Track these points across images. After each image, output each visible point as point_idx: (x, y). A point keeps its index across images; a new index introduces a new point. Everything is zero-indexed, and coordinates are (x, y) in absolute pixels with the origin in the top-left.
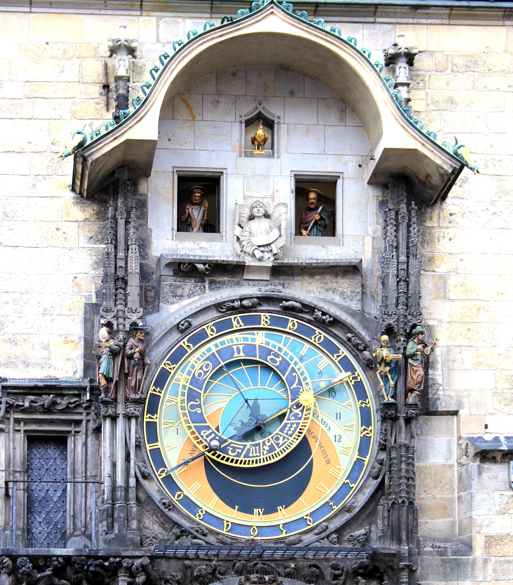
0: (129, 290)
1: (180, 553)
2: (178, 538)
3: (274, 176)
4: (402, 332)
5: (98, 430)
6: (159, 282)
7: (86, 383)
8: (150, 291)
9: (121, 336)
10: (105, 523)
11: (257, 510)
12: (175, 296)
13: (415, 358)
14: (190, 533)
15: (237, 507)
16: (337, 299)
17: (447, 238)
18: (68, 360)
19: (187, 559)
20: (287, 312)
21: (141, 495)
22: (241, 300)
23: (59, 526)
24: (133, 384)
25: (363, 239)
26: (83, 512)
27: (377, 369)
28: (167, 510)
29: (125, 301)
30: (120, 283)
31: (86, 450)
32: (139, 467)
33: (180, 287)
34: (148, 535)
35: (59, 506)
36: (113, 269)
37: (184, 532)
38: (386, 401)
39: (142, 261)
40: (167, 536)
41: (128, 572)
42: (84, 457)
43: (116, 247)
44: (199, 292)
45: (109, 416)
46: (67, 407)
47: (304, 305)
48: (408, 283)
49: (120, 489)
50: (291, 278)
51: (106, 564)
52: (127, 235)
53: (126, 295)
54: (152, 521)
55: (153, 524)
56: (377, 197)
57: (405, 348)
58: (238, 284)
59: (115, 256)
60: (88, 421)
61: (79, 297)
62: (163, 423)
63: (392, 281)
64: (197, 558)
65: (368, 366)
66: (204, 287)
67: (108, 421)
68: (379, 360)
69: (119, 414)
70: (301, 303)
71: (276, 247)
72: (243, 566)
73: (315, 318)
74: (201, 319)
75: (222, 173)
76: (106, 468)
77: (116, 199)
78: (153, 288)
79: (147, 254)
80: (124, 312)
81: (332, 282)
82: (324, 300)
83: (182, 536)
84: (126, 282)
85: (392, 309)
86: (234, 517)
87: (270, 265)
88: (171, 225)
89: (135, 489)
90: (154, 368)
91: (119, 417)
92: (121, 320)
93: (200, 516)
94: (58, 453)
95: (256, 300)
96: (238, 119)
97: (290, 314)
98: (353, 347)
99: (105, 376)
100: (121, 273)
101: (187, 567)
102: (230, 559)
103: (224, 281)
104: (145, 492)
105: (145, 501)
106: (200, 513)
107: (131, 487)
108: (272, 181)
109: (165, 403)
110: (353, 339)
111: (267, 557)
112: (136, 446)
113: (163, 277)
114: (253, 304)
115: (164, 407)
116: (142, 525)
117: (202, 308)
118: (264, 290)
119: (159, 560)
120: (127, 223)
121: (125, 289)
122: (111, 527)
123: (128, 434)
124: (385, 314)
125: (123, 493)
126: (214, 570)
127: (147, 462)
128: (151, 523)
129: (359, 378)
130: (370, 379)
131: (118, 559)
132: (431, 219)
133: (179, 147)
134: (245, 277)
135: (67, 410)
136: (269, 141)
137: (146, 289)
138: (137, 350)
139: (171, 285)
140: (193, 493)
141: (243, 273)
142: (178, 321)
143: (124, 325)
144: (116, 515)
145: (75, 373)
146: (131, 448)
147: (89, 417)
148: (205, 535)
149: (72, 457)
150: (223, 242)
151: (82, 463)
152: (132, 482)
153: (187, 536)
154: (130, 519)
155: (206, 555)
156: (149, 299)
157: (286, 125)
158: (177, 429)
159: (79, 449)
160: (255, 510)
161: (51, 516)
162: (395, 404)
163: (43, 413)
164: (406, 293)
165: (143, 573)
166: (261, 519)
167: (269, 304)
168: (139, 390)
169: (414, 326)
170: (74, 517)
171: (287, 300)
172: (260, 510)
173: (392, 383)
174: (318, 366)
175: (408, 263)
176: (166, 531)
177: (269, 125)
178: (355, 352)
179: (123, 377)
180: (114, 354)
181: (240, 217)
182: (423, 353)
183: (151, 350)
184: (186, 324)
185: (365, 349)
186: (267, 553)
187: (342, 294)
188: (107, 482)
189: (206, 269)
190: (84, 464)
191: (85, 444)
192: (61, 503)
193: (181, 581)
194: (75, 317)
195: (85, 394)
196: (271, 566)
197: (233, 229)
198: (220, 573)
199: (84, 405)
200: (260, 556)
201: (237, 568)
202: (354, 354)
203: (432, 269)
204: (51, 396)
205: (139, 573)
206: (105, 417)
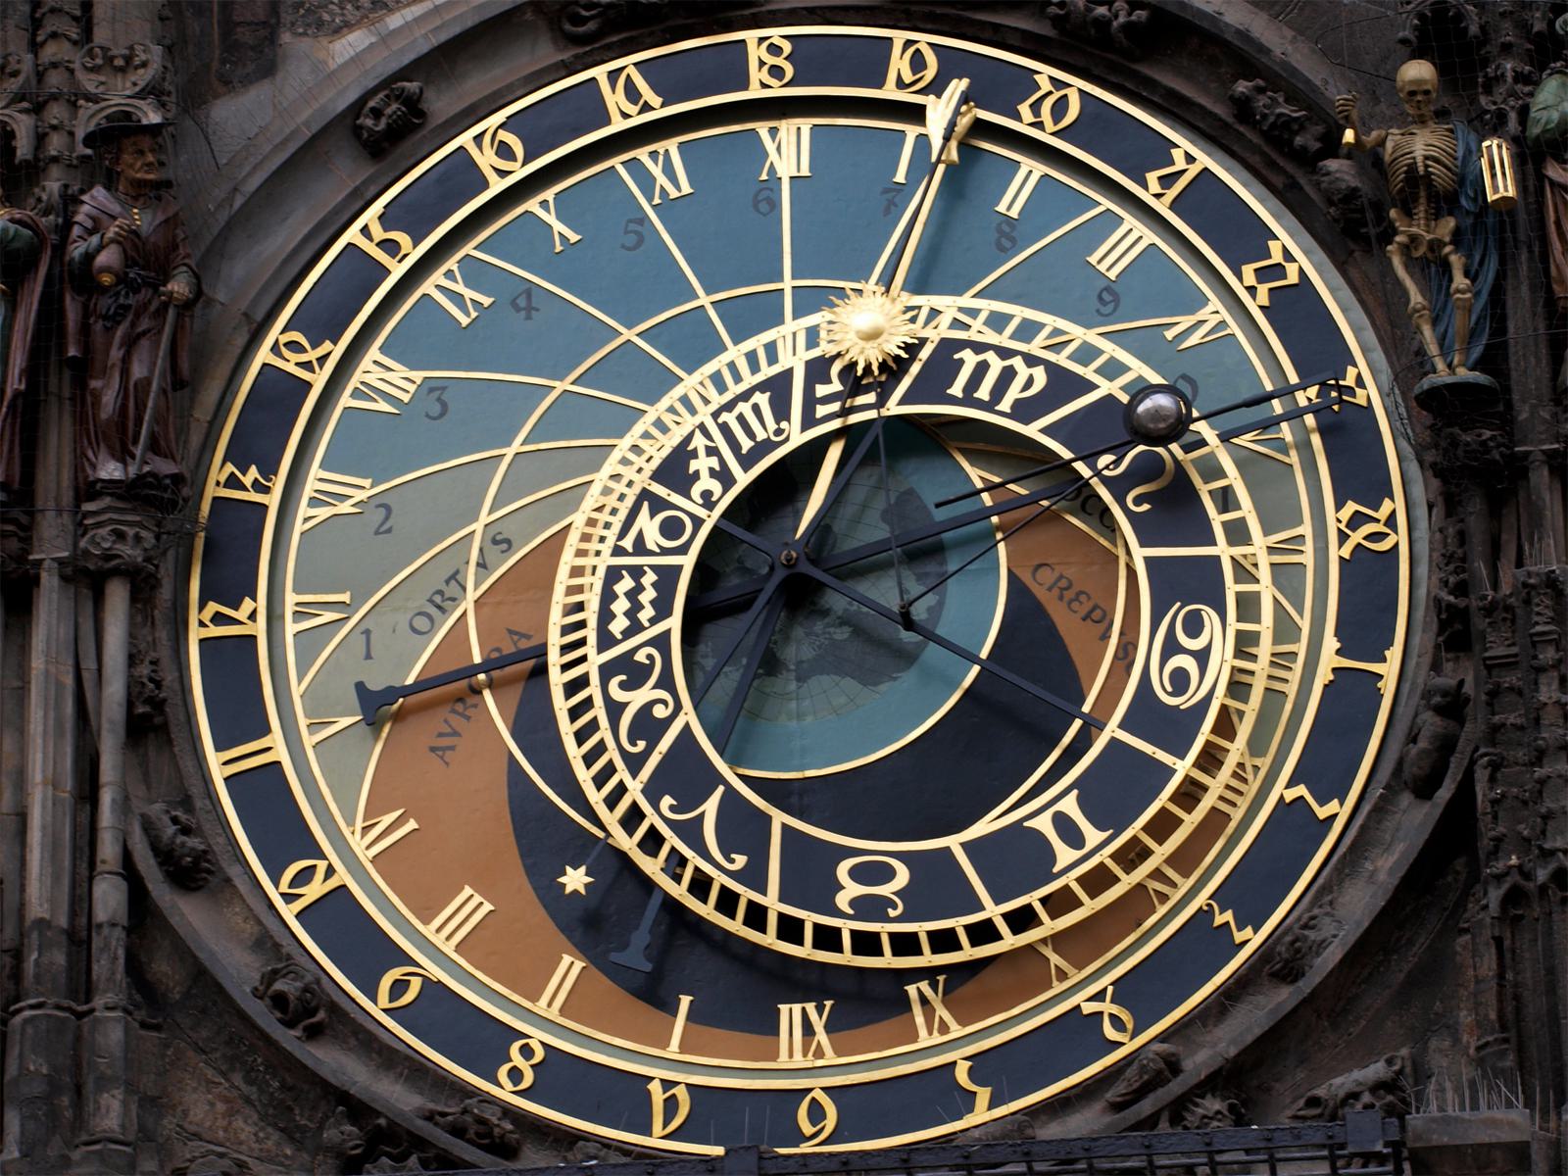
4: (1508, 34)
9: (52, 186)
11: (797, 1008)
14: (419, 1143)
15: (685, 1001)
21: (164, 969)
27: (1388, 234)
32: (148, 826)
49: (35, 935)
54: (227, 1100)
55: (230, 1113)
89: (119, 934)
90: (241, 340)
91: (36, 581)
92: (56, 112)
93: (515, 1075)
98: (1266, 149)
104: (183, 952)
106: (517, 1060)
107: (100, 926)
109: (303, 510)
110: (1262, 101)
115: (299, 527)
116: (168, 1123)
117: (470, 24)
123: (89, 664)
125: (59, 958)
127: (198, 804)
128: (220, 1107)
129: (1292, 270)
130: (1370, 299)
140: (449, 949)
142: (352, 96)
143: (71, 134)
146: (105, 726)
152: (109, 898)
154: (89, 1086)
156: (244, 35)
158: (367, 632)
160: (784, 1008)
166: (819, 1053)
172: (811, 1007)
174: (1093, 259)
178: (1282, 171)
179: (59, 383)
183: (219, 248)
184: (394, 106)
202: (1279, 181)
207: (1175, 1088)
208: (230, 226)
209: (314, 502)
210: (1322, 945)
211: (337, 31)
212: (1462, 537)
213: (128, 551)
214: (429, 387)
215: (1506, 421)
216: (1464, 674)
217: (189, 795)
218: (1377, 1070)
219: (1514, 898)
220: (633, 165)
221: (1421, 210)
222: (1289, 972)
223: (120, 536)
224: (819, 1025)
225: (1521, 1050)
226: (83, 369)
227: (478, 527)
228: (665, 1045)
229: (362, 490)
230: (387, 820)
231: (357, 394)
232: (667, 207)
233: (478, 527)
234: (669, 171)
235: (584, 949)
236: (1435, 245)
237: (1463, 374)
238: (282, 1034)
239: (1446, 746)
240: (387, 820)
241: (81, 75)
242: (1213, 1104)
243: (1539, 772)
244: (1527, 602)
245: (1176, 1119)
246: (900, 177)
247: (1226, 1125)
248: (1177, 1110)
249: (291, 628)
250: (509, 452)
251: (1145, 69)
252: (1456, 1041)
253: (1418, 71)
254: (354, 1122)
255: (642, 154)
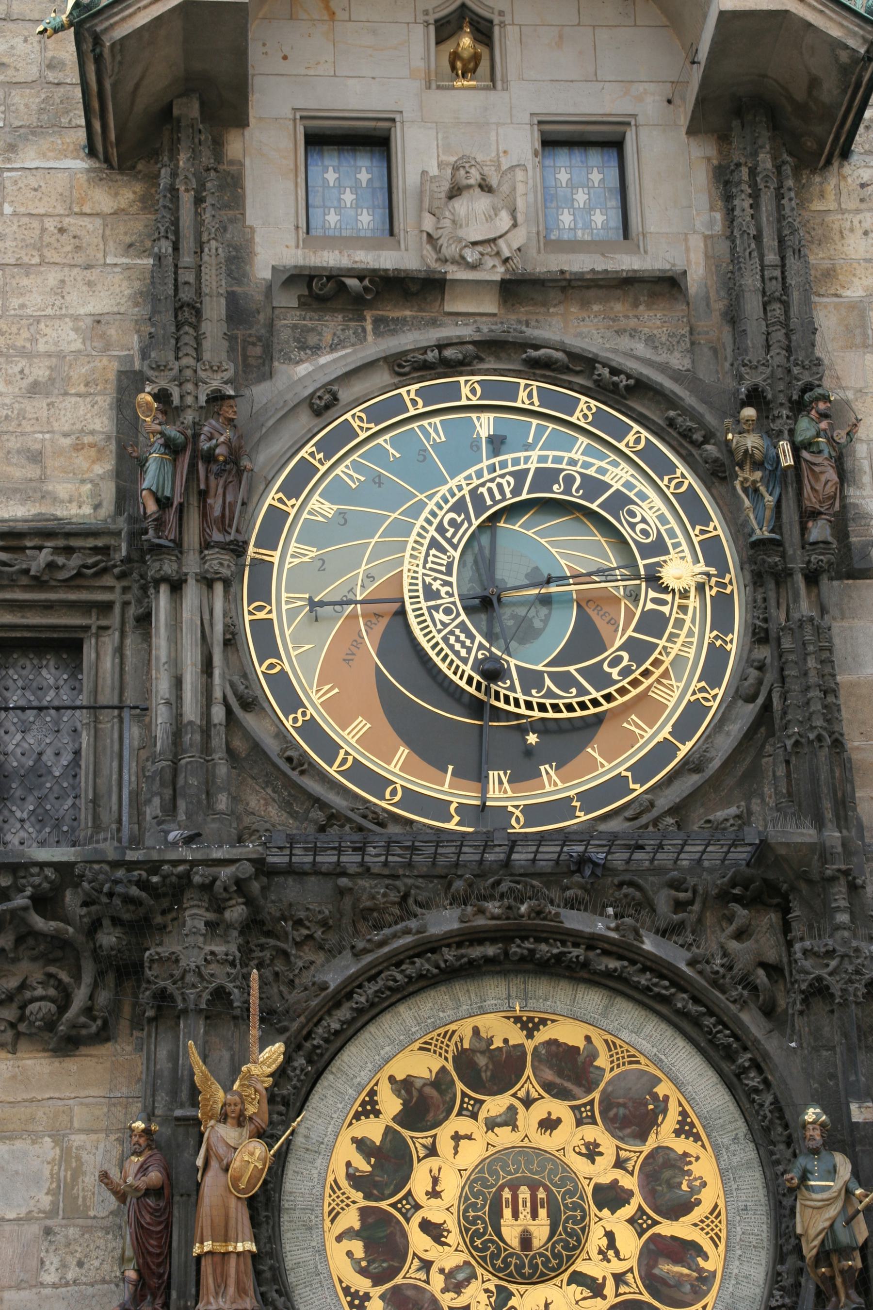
0: (206, 327)
1: (328, 859)
2: (322, 829)
3: (498, 124)
4: (782, 399)
5: (145, 620)
6: (271, 326)
7: (122, 524)
8: (254, 344)
9: (189, 417)
10: (157, 801)
12: (303, 347)
13: (814, 449)
14: (349, 820)
15: (451, 768)
16: (640, 348)
17: (861, 232)
18: (83, 481)
19: (344, 874)
20: (538, 372)
21: (238, 744)
22: (440, 347)
23: (65, 828)
24: (217, 512)
25: (686, 240)
26: (115, 789)
28: (296, 773)
29: (198, 349)
30: (186, 314)
31: (122, 663)
32: (232, 685)
33: (313, 330)
34: (254, 827)
35: (65, 785)
36: (171, 286)
37: (334, 817)
38: (758, 534)
39: (235, 288)
40: (298, 828)
41: (206, 898)
42: (117, 676)
43: (176, 249)
44: (353, 339)
45: (165, 579)
46: (79, 575)
47: (573, 356)
48: (786, 306)
50: (542, 310)
51: (155, 879)
52: (199, 223)
53: (198, 340)
55: (266, 804)
56: (709, 159)
57: (792, 432)
58: (434, 323)
59: (176, 266)
60: (126, 604)
61: (105, 361)
62: (284, 599)
63: (752, 305)
64: (366, 871)
65: (714, 474)
66: (364, 330)
67: (164, 589)
68: (739, 456)
69: (186, 574)
70: (565, 351)
71: (509, 246)
72: (470, 885)
73: (595, 381)
74: (358, 388)
75: (393, 120)
76: (163, 686)
77: (173, 155)
78: (259, 339)
79: (245, 275)
80: (195, 371)
81: (627, 317)
82: (615, 351)
83: (332, 826)
84: (198, 313)
85: (755, 354)
86: (446, 788)
87: (498, 278)
88: (292, 219)
89: (223, 729)
90: (262, 487)
91: (186, 581)
92: (189, 387)
94: (65, 677)
95: (470, 347)
96: (421, 18)
97: (544, 376)
99: (154, 494)
100: (186, 295)
101: (342, 892)
102: (439, 871)
103: (404, 321)
104: (247, 735)
105: (248, 755)
108: (493, 135)
109: (288, 559)
111: (521, 867)
112: (227, 643)
113: (277, 312)
114: (465, 357)
115: (287, 566)
116: (240, 808)
118: (486, 329)
119: (281, 879)
120: (199, 200)
121: (196, 328)
122: (170, 809)
123: (206, 617)
124: (745, 365)
125: (197, 737)
126: (405, 897)
131: (181, 868)
132: (822, 195)
133: (303, 71)
134: (448, 308)
135: (77, 580)
136: (485, 64)
137: (244, 341)
138: (222, 439)
139: (294, 327)
141: (443, 299)
142: (310, 390)
144: (181, 782)
145: (97, 507)
147: (128, 597)
148: (381, 824)
149: (92, 678)
150: (399, 249)
151: (113, 689)
152: (218, 713)
153: (342, 826)
155: (386, 864)
157: (517, 28)
159: (108, 663)
161: (48, 807)
162: (778, 543)
163: (26, 588)
164: (786, 324)
165: (241, 900)
166: (505, 792)
167: (498, 358)
168: (230, 526)
169: (808, 388)
170: (95, 802)
171: (537, 347)
173: (770, 500)
175: (783, 266)
176: (295, 819)
177: (484, 32)
179: (194, 500)
180: (173, 449)
181: (432, 198)
182: (831, 440)
185: (706, 441)
186: (521, 856)
187: (650, 340)
188: (161, 716)
189: (366, 289)
190: (116, 692)
191: (120, 650)
192: (71, 780)
193: (331, 922)
194: (98, 398)
195: (118, 548)
196: (533, 887)
197: (420, 219)
198: (421, 905)
199: (116, 571)
200: (507, 864)
201: (458, 891)
202: (684, 452)
203: (833, 291)
204: (45, 551)
205: (230, 899)
206: (157, 582)
207: (655, 813)
208: (259, 441)
209: (293, 556)
210: (712, 759)
211: (298, 363)
212: (765, 600)
213: (225, 572)
214: (340, 513)
215: (783, 556)
216: (764, 653)
217: (247, 675)
218: (733, 810)
219: (797, 744)
220: (421, 427)
221: (747, 467)
222: (697, 769)
223: (221, 564)
224: (505, 780)
225: (800, 806)
226: (203, 495)
227: (361, 570)
228: (443, 785)
229: (313, 552)
230: (327, 687)
231: (310, 513)
232: (435, 446)
233: (361, 570)
234: (436, 430)
235: (409, 744)
236: (754, 482)
237: (767, 535)
238: (288, 772)
239: (760, 682)
240: (327, 687)
241: (200, 372)
242: (670, 820)
243: (810, 695)
244: (801, 627)
245: (655, 825)
246: (530, 440)
247: (675, 829)
248: (655, 822)
249: (285, 607)
250: (373, 541)
251: (629, 403)
252: (763, 800)
253: (749, 412)
254: (321, 809)
255: (425, 423)
